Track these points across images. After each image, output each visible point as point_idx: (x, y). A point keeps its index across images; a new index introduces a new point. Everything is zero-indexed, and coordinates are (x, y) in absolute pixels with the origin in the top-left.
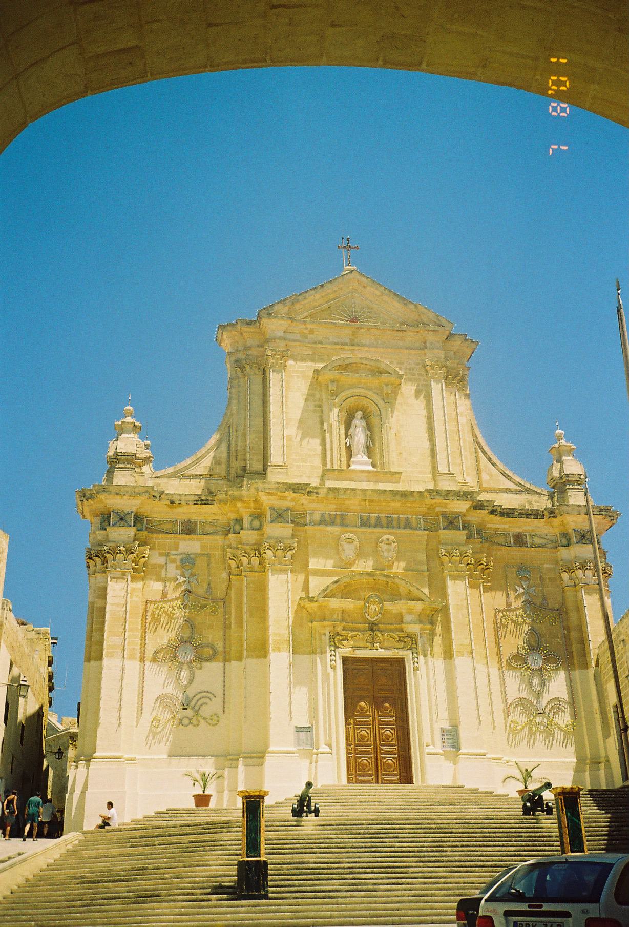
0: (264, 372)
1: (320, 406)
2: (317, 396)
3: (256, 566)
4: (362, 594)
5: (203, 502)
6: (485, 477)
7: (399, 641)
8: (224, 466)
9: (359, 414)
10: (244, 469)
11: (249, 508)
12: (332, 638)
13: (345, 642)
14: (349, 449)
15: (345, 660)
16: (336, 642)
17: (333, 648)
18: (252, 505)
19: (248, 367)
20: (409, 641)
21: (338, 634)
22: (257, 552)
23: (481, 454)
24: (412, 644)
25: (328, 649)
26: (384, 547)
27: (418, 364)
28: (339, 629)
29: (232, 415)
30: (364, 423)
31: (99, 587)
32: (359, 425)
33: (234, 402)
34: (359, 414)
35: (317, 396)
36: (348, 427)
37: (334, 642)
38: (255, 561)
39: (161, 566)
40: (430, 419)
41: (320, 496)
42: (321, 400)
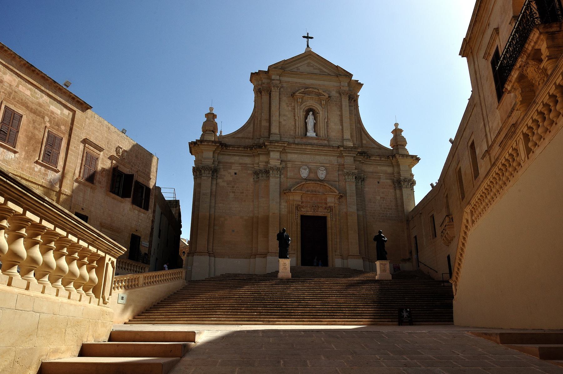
0: (270, 94)
1: (294, 109)
2: (293, 105)
6: (364, 142)
9: (311, 113)
13: (302, 209)
17: (297, 211)
19: (263, 92)
23: (362, 132)
24: (331, 210)
32: (311, 119)
34: (311, 113)
35: (293, 105)
36: (306, 118)
37: (297, 209)
40: (341, 116)
42: (294, 106)
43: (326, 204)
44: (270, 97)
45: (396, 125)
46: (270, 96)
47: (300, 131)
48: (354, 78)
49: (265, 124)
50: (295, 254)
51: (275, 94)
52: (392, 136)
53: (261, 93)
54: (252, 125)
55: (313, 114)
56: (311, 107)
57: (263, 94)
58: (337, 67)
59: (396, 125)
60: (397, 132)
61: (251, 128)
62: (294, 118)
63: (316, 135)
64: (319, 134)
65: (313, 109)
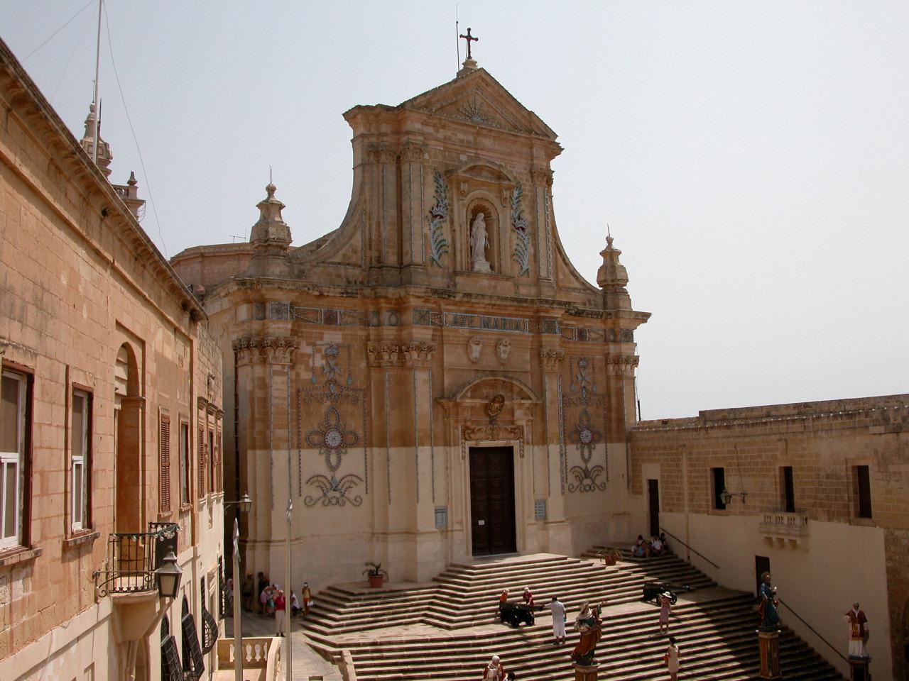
3: (395, 361)
4: (485, 391)
5: (349, 295)
6: (561, 276)
7: (511, 432)
8: (359, 254)
9: (482, 215)
10: (379, 260)
11: (390, 304)
12: (464, 433)
13: (472, 435)
14: (471, 249)
15: (472, 449)
16: (466, 435)
17: (464, 441)
18: (394, 301)
20: (517, 432)
21: (467, 428)
22: (397, 348)
23: (559, 256)
25: (460, 441)
26: (502, 348)
27: (525, 169)
28: (469, 424)
29: (365, 201)
30: (483, 225)
31: (258, 378)
33: (367, 187)
34: (482, 215)
38: (394, 357)
39: (309, 356)
41: (457, 299)
43: (513, 422)
44: (399, 170)
45: (609, 240)
46: (397, 167)
47: (461, 258)
48: (556, 141)
49: (388, 232)
50: (462, 530)
51: (412, 169)
52: (600, 261)
53: (377, 154)
54: (358, 236)
55: (485, 219)
56: (482, 203)
57: (383, 157)
58: (531, 113)
59: (609, 240)
60: (610, 255)
61: (357, 240)
62: (451, 228)
63: (492, 267)
64: (496, 265)
65: (485, 206)
